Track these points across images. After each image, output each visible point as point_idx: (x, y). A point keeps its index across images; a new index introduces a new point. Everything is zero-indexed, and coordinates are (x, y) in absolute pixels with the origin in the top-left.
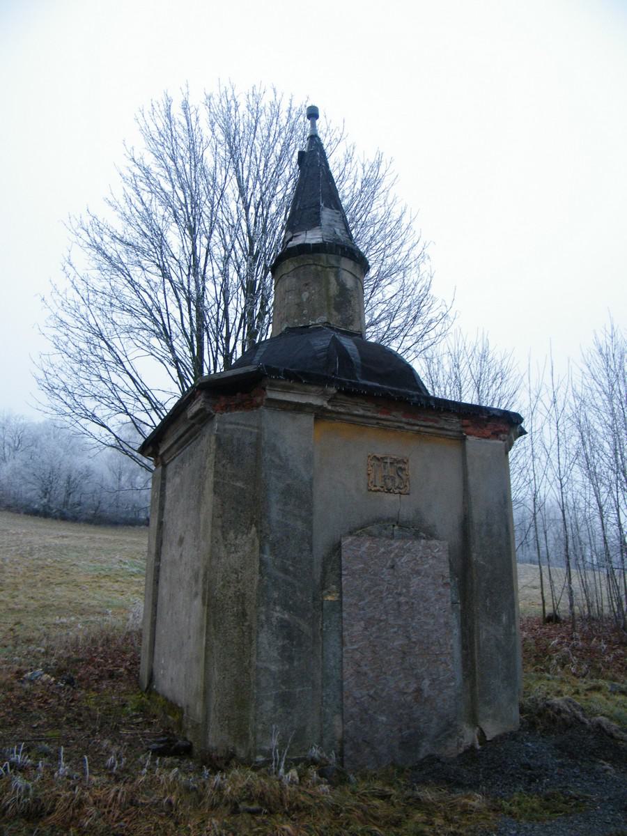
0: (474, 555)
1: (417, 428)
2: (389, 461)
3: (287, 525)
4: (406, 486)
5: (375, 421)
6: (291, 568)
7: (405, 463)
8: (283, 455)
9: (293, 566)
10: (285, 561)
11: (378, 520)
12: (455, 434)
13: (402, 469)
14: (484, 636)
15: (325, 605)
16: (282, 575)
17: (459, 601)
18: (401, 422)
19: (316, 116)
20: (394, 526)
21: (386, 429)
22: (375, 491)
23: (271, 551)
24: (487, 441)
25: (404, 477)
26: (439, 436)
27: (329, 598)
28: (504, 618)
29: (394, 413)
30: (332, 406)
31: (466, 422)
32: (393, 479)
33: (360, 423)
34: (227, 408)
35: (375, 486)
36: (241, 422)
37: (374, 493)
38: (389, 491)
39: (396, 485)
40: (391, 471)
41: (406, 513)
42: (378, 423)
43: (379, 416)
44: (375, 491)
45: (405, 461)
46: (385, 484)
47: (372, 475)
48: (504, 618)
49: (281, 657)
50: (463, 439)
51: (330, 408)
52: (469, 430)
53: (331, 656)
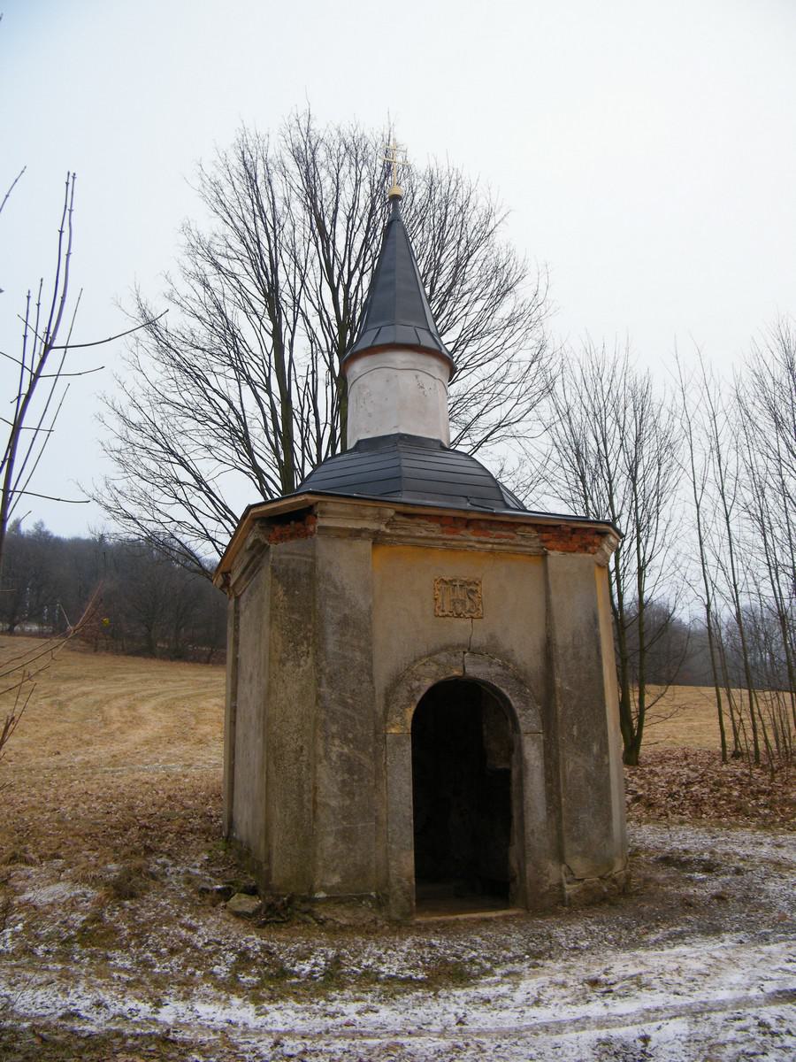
0: (558, 680)
2: (458, 584)
3: (344, 657)
4: (479, 609)
5: (441, 542)
6: (350, 701)
7: (477, 585)
8: (339, 584)
9: (352, 698)
10: (343, 694)
11: (445, 648)
12: (535, 550)
14: (570, 767)
15: (388, 738)
16: (340, 708)
17: (541, 731)
18: (470, 541)
20: (464, 653)
21: (453, 549)
22: (443, 616)
23: (328, 683)
24: (573, 555)
25: (476, 600)
26: (515, 553)
27: (393, 731)
28: (595, 749)
29: (462, 532)
30: (391, 529)
31: (545, 536)
32: (463, 603)
33: (424, 546)
34: (281, 538)
35: (443, 611)
36: (295, 551)
37: (442, 619)
38: (459, 616)
39: (467, 608)
40: (460, 594)
41: (479, 638)
42: (444, 544)
43: (445, 536)
44: (443, 616)
45: (477, 582)
46: (455, 609)
47: (440, 600)
48: (595, 749)
49: (341, 791)
50: (545, 555)
51: (388, 531)
52: (549, 545)
53: (396, 790)
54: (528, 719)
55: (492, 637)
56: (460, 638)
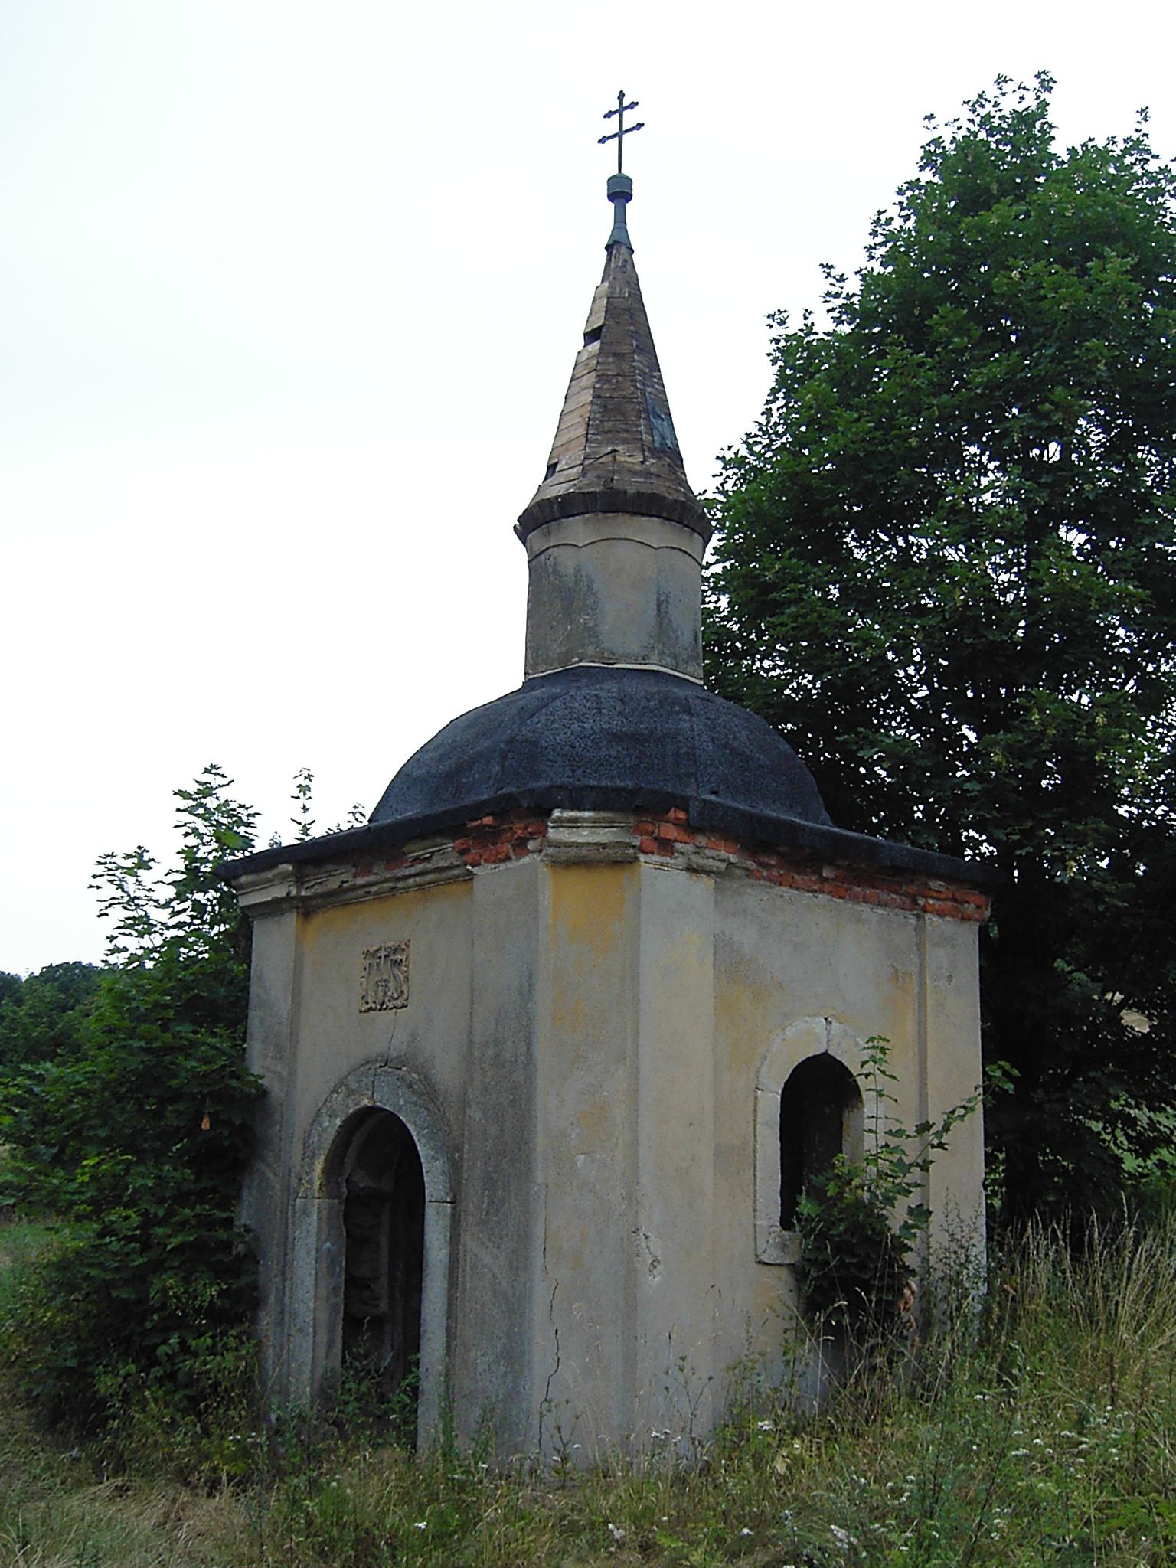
1: (411, 881)
2: (382, 954)
5: (361, 892)
13: (397, 963)
19: (628, 197)
21: (380, 897)
22: (367, 1011)
24: (509, 865)
26: (448, 882)
41: (400, 1042)
45: (403, 946)
54: (434, 1182)
55: (414, 1037)
56: (379, 1047)
